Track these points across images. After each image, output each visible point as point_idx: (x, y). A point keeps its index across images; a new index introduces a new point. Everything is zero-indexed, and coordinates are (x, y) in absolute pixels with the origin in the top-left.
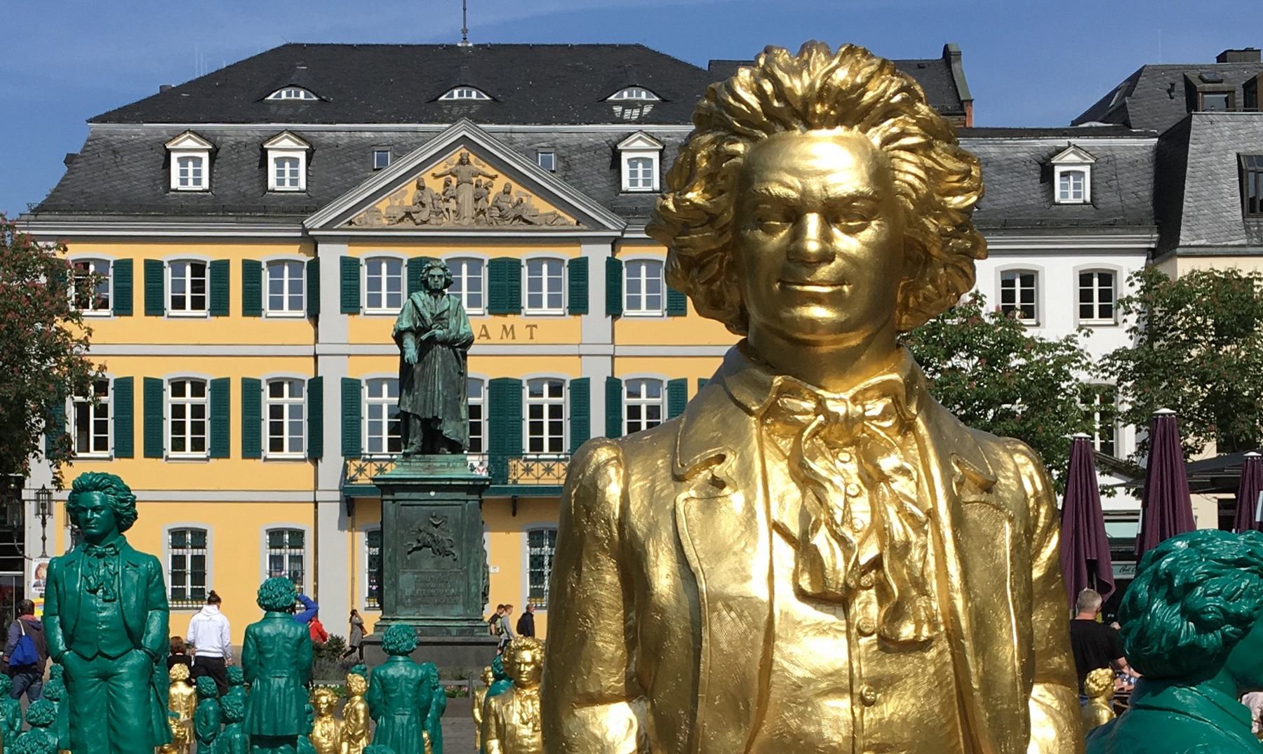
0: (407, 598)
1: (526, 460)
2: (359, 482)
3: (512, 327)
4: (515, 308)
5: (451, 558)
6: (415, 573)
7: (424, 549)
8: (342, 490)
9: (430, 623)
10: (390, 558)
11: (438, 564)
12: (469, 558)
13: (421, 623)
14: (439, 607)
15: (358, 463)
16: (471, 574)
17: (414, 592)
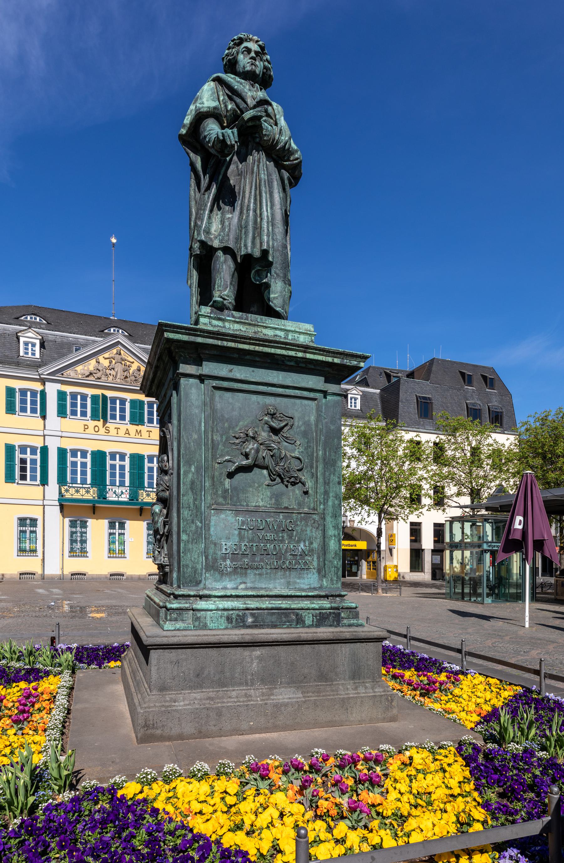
0: (224, 559)
1: (146, 491)
2: (66, 496)
3: (140, 431)
4: (142, 422)
5: (297, 490)
6: (237, 512)
7: (256, 470)
8: (59, 500)
9: (266, 604)
10: (193, 483)
11: (277, 497)
12: (326, 493)
13: (253, 604)
14: (280, 573)
15: (66, 487)
16: (329, 519)
17: (238, 546)
